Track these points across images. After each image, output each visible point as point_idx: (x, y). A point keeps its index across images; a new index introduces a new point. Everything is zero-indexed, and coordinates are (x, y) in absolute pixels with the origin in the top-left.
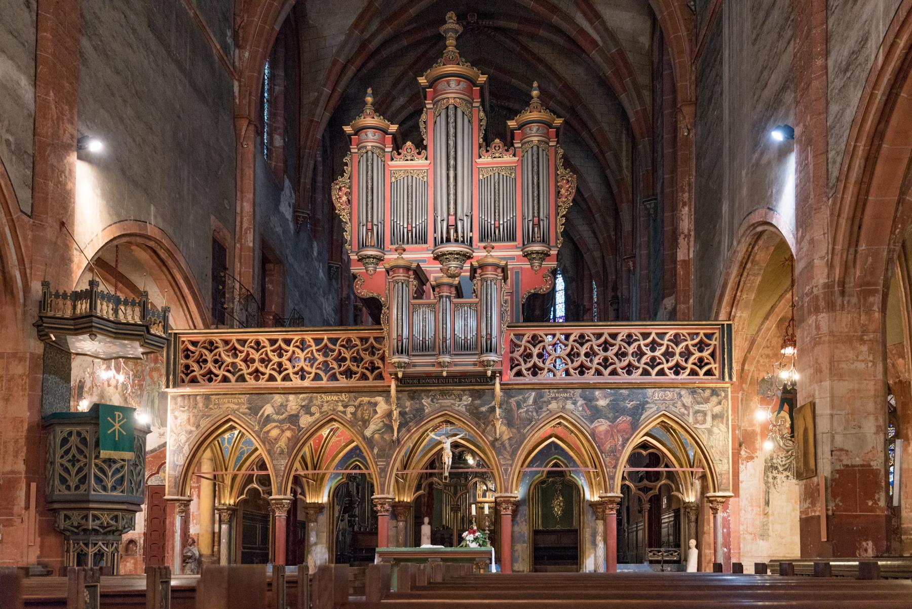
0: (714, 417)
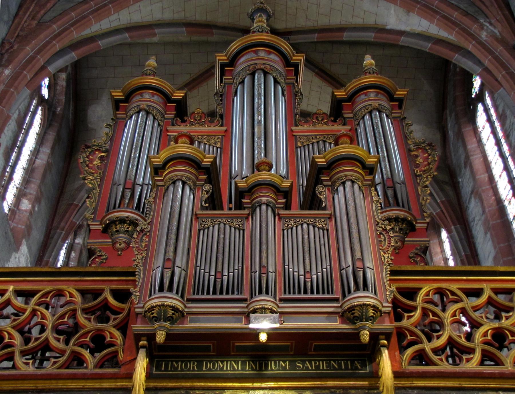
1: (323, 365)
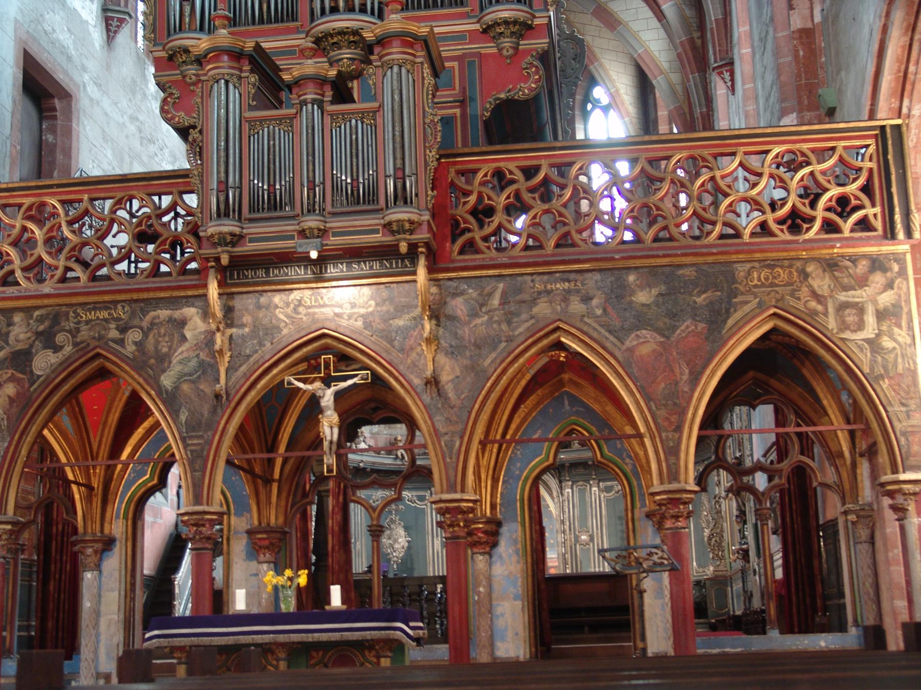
0: (881, 315)
1: (376, 265)
